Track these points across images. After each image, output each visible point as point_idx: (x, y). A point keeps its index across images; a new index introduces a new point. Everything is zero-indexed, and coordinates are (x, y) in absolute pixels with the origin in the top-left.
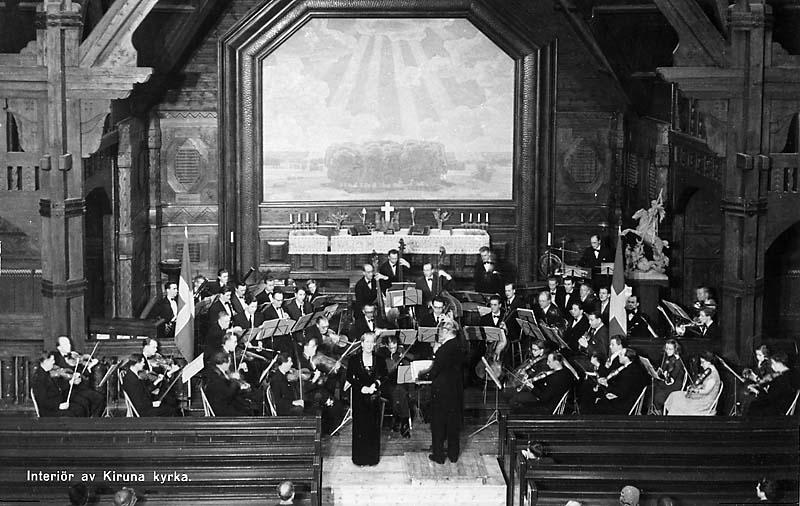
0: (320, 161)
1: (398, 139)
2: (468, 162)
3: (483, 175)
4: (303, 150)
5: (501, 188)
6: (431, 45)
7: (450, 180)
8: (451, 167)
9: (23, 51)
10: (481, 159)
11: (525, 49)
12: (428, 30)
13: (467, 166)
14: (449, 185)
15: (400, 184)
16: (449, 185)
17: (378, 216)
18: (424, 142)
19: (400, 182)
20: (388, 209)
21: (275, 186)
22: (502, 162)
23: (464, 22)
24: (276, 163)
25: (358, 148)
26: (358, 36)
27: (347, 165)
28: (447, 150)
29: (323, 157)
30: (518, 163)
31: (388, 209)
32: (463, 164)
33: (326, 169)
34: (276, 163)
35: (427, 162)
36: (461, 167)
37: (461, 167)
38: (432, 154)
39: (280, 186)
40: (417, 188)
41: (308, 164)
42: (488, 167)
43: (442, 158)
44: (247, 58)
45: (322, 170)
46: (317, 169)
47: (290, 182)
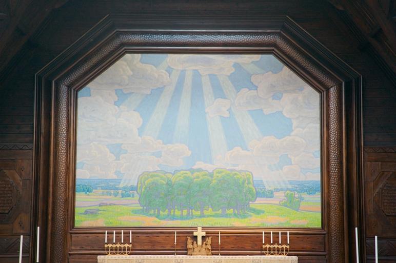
0: (132, 188)
1: (209, 167)
2: (277, 190)
3: (291, 203)
4: (115, 177)
5: (309, 215)
6: (241, 80)
7: (258, 208)
8: (258, 195)
10: (290, 187)
11: (329, 82)
12: (236, 65)
13: (276, 194)
14: (258, 212)
15: (210, 211)
16: (258, 212)
17: (190, 241)
18: (232, 170)
19: (210, 209)
20: (200, 233)
21: (86, 212)
22: (310, 191)
23: (271, 58)
24: (87, 190)
25: (170, 176)
26: (169, 70)
27: (157, 193)
29: (135, 185)
30: (326, 191)
31: (200, 233)
32: (272, 192)
33: (137, 197)
35: (238, 192)
36: (271, 195)
37: (271, 195)
38: (241, 181)
39: (92, 213)
40: (226, 216)
41: (120, 192)
42: (297, 196)
43: (251, 186)
44: (64, 88)
45: (133, 196)
46: (129, 196)
47: (104, 208)
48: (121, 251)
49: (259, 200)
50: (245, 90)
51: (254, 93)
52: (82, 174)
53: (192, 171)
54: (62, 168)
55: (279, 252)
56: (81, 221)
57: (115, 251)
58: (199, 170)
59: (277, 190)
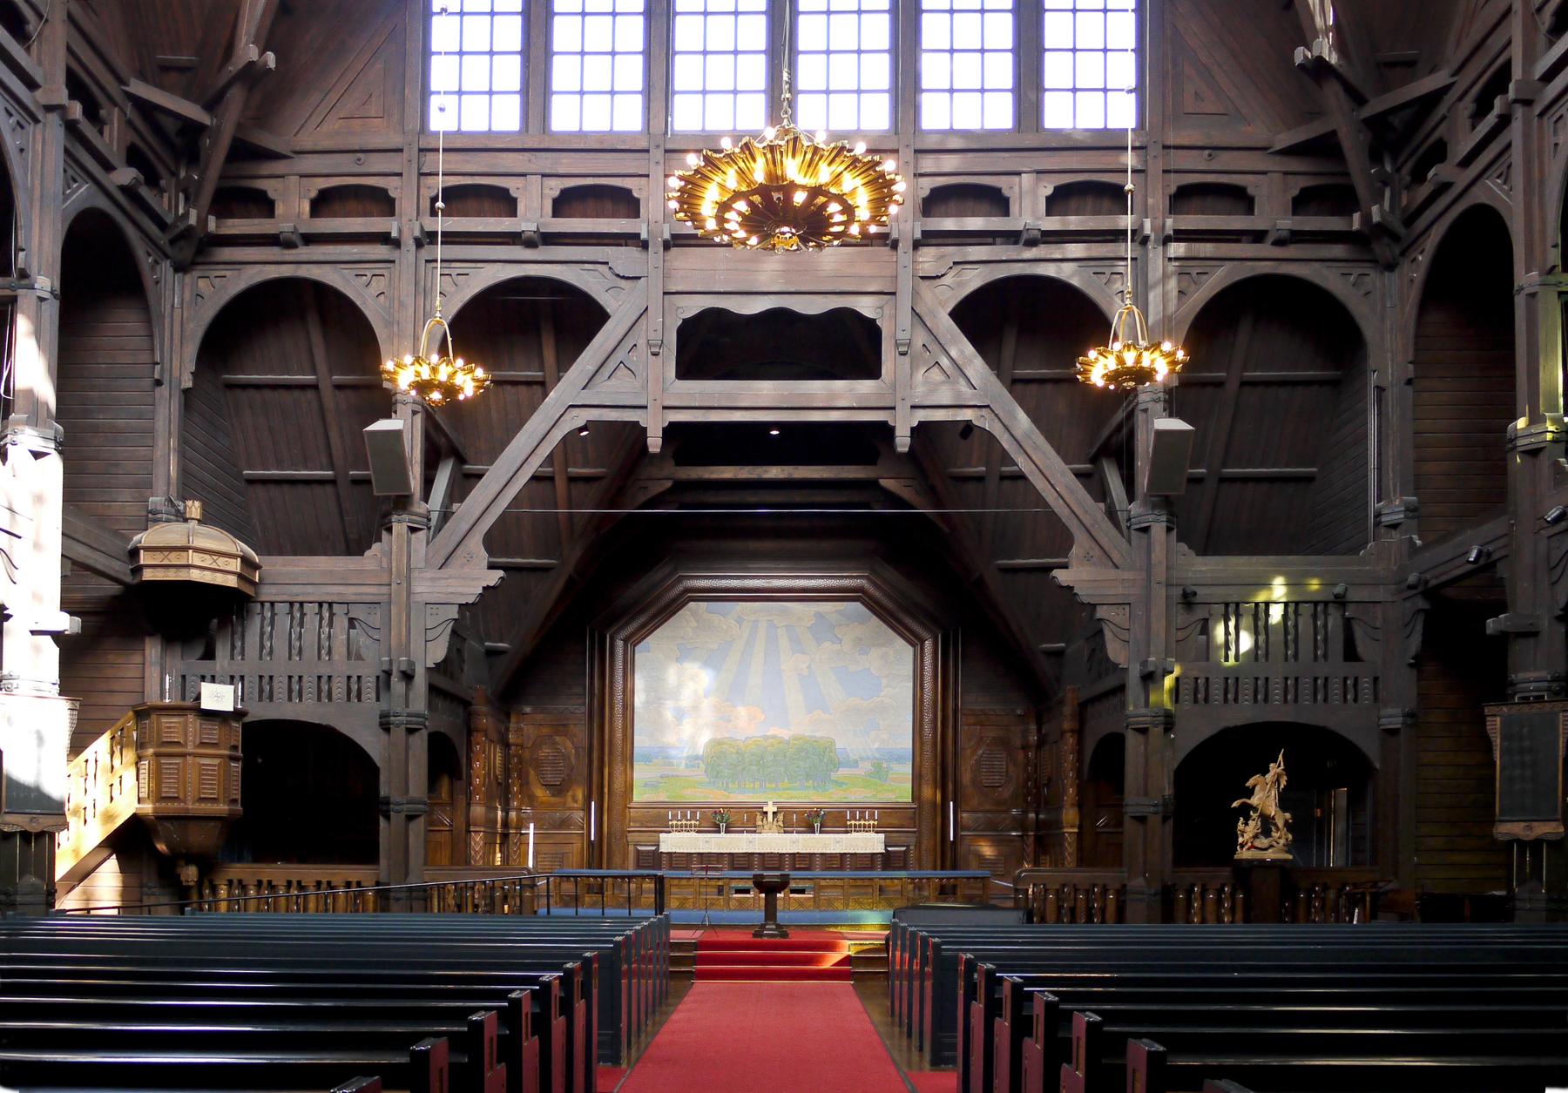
1: (785, 734)
9: (368, 553)
14: (839, 784)
16: (839, 784)
17: (759, 817)
20: (770, 809)
21: (646, 785)
22: (899, 759)
24: (647, 759)
26: (739, 621)
28: (839, 745)
31: (770, 809)
33: (702, 766)
34: (647, 759)
35: (817, 758)
36: (855, 764)
48: (687, 828)
49: (842, 771)
50: (827, 644)
51: (836, 647)
52: (641, 741)
53: (766, 738)
54: (619, 734)
55: (866, 829)
56: (640, 795)
57: (680, 829)
58: (774, 737)
59: (862, 759)
